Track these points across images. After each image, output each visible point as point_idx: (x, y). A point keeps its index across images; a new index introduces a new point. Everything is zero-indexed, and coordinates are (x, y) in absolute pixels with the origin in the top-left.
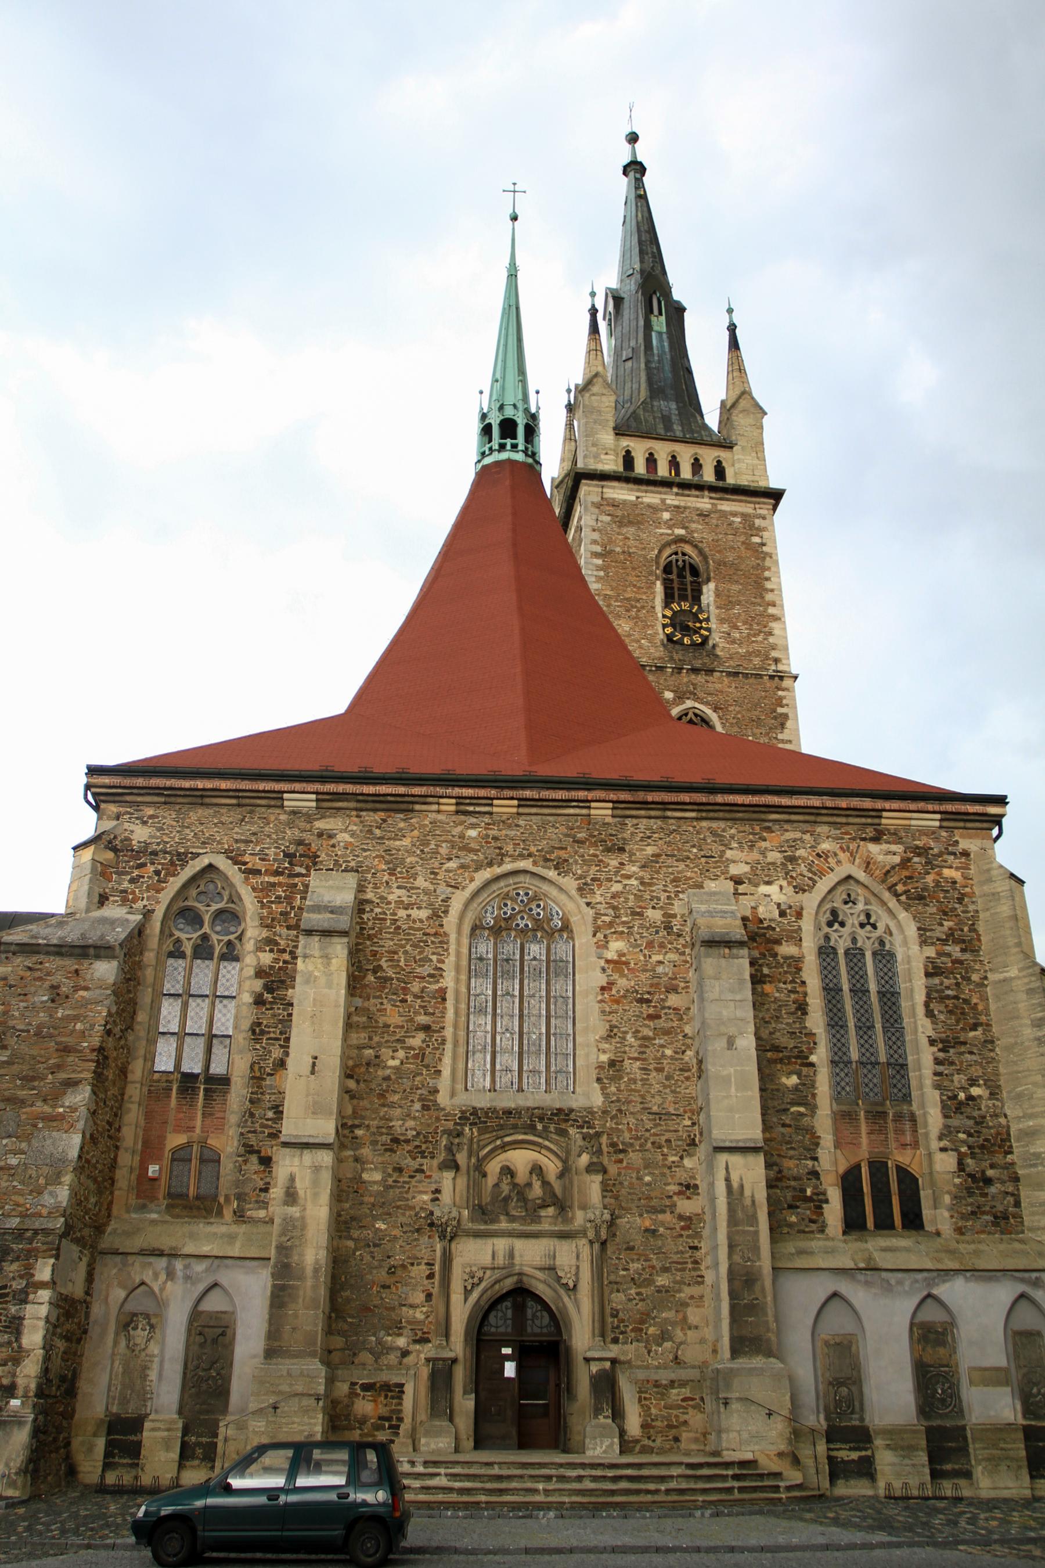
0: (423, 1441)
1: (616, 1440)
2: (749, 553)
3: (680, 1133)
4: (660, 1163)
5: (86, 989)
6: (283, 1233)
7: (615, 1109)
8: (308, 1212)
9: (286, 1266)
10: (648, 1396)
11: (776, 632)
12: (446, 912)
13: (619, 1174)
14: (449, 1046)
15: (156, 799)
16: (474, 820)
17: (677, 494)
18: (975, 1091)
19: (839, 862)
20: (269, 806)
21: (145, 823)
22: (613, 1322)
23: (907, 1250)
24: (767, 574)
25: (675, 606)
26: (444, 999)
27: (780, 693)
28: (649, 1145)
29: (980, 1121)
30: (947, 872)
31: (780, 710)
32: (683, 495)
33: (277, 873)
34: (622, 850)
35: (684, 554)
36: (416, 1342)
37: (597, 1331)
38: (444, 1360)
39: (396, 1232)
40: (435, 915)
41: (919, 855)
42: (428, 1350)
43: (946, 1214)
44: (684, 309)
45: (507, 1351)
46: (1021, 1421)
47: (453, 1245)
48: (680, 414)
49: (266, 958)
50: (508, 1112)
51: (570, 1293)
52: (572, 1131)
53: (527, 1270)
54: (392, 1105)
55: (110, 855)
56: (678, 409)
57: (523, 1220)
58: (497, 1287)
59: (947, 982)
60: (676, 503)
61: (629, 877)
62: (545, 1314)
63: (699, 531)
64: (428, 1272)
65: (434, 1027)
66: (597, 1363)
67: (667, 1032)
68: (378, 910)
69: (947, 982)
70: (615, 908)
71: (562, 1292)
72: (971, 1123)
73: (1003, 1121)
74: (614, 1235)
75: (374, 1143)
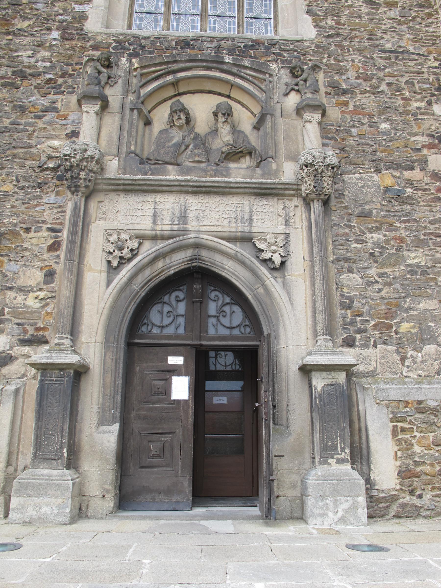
0: (14, 502)
1: (362, 500)
3: (426, 76)
4: (401, 109)
10: (406, 425)
13: (344, 119)
22: (344, 317)
28: (383, 87)
36: (24, 342)
37: (320, 327)
38: (61, 368)
42: (41, 355)
45: (176, 360)
47: (93, 205)
51: (276, 274)
52: (273, 66)
53: (206, 238)
54: (19, 33)
58: (160, 264)
62: (236, 308)
64: (51, 242)
66: (324, 374)
71: (263, 271)
74: (340, 195)
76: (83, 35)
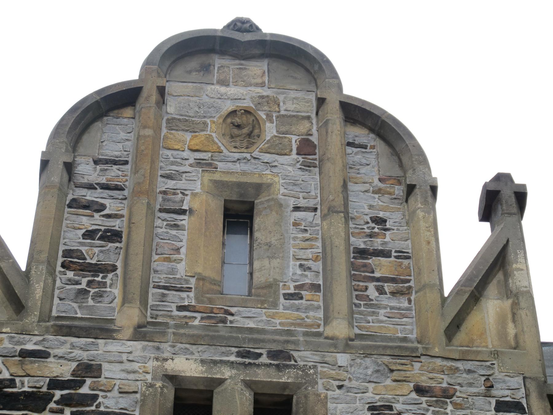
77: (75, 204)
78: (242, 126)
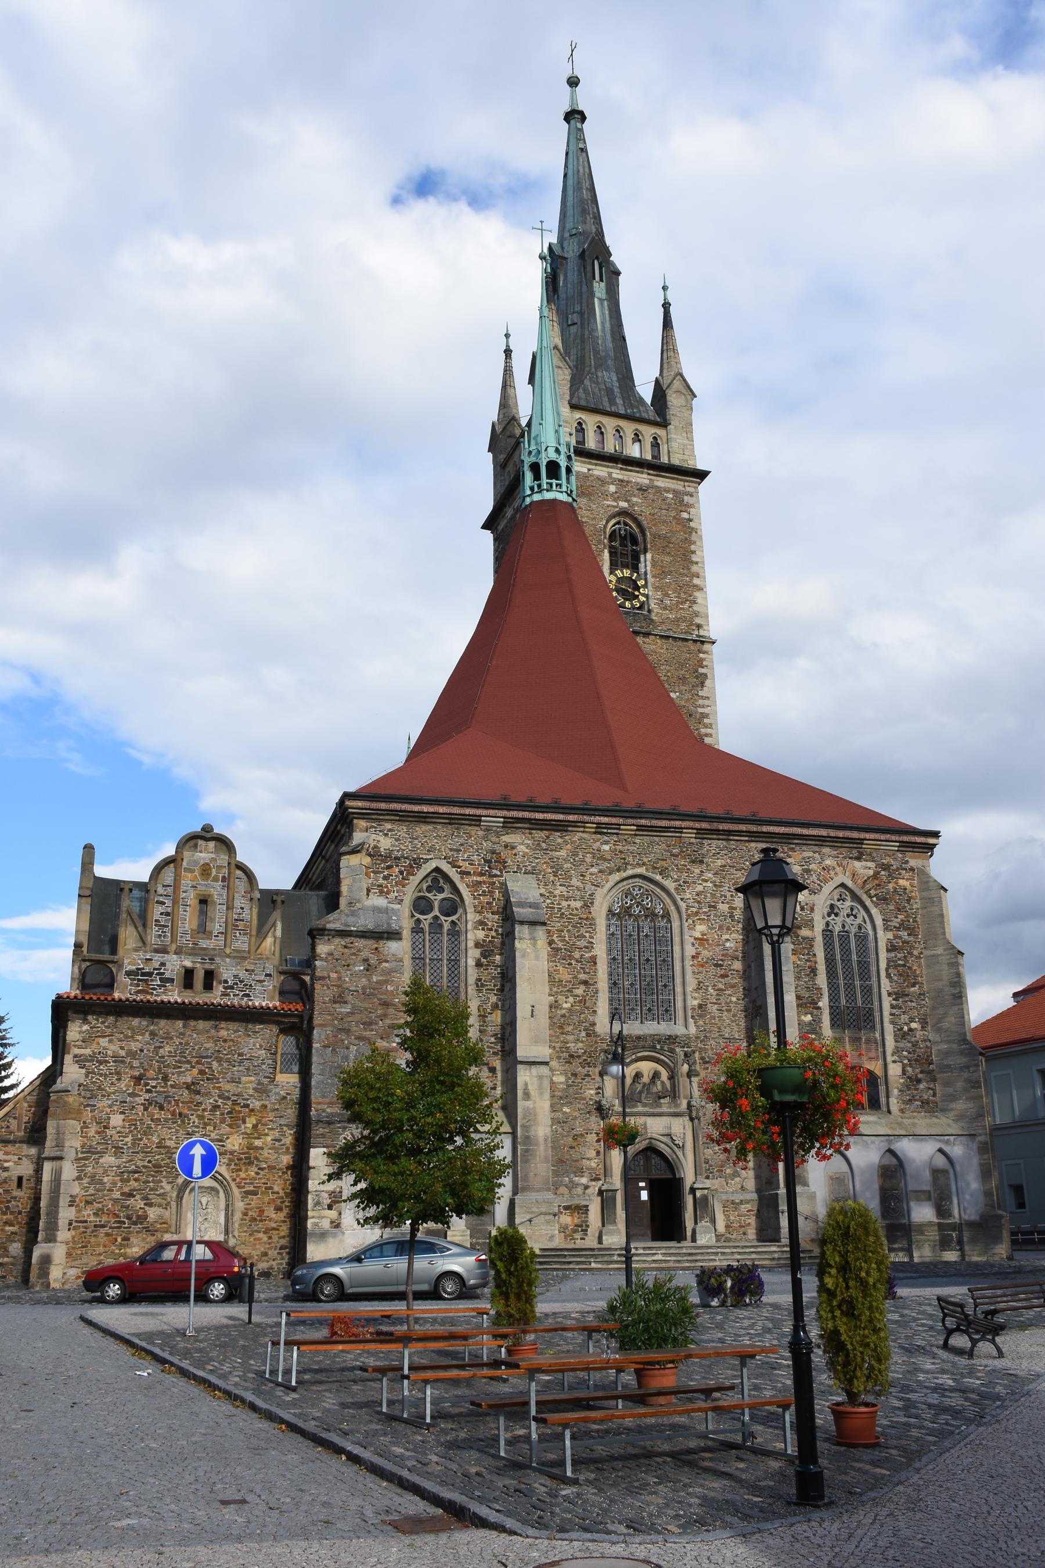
0: (604, 1238)
2: (679, 527)
5: (387, 961)
6: (524, 1118)
7: (704, 1036)
8: (537, 1105)
9: (528, 1137)
11: (699, 601)
12: (592, 903)
14: (600, 995)
15: (393, 818)
16: (606, 838)
17: (621, 469)
18: (914, 1025)
19: (836, 873)
20: (470, 825)
21: (386, 835)
23: (875, 1123)
24: (693, 547)
25: (619, 573)
26: (595, 963)
27: (701, 655)
29: (915, 1044)
30: (901, 882)
31: (701, 670)
32: (626, 470)
33: (481, 874)
34: (701, 862)
35: (626, 524)
36: (592, 1180)
39: (576, 1114)
40: (586, 906)
41: (884, 870)
43: (895, 1101)
44: (618, 273)
45: (642, 1184)
46: (936, 1221)
48: (620, 387)
49: (481, 934)
50: (639, 1038)
52: (678, 1050)
53: (655, 1136)
55: (369, 859)
56: (619, 380)
57: (651, 1106)
59: (899, 955)
60: (620, 477)
61: (706, 881)
63: (638, 504)
65: (591, 982)
67: (733, 986)
68: (548, 901)
69: (899, 955)
70: (699, 902)
72: (910, 1045)
73: (928, 1044)
75: (559, 1058)
76: (597, 1036)
77: (158, 902)
78: (205, 870)
